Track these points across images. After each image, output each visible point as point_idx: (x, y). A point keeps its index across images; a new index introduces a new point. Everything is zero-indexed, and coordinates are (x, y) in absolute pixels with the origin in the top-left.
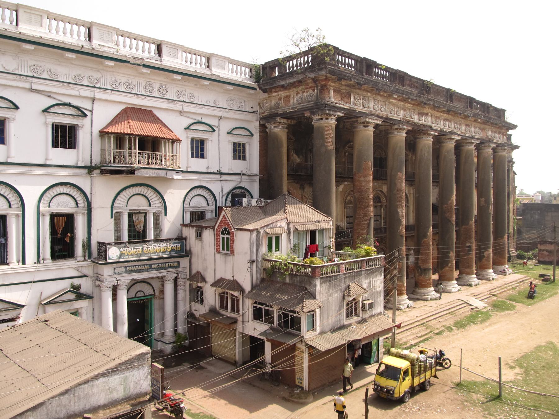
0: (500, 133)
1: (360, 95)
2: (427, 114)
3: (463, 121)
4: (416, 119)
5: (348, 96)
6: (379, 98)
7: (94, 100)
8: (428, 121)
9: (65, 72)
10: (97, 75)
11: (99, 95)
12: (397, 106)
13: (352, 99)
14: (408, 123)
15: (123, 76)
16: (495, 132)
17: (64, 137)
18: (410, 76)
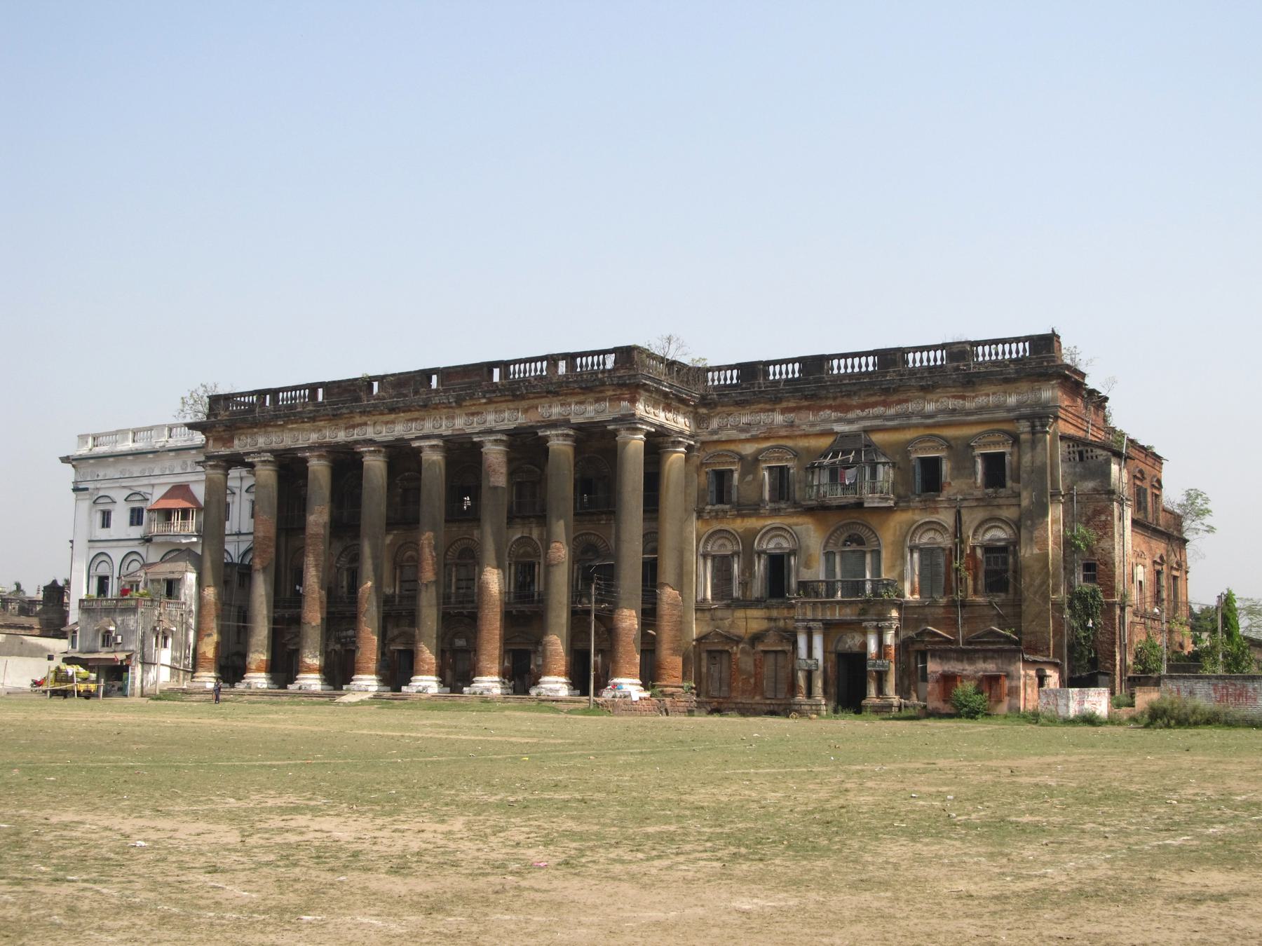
0: (598, 400)
1: (246, 435)
2: (365, 424)
3: (457, 411)
4: (342, 436)
5: (231, 440)
6: (270, 429)
7: (153, 485)
8: (370, 432)
9: (136, 470)
10: (152, 466)
11: (153, 481)
12: (304, 430)
13: (236, 442)
14: (321, 446)
15: (168, 463)
16: (581, 403)
17: (136, 517)
18: (334, 382)
